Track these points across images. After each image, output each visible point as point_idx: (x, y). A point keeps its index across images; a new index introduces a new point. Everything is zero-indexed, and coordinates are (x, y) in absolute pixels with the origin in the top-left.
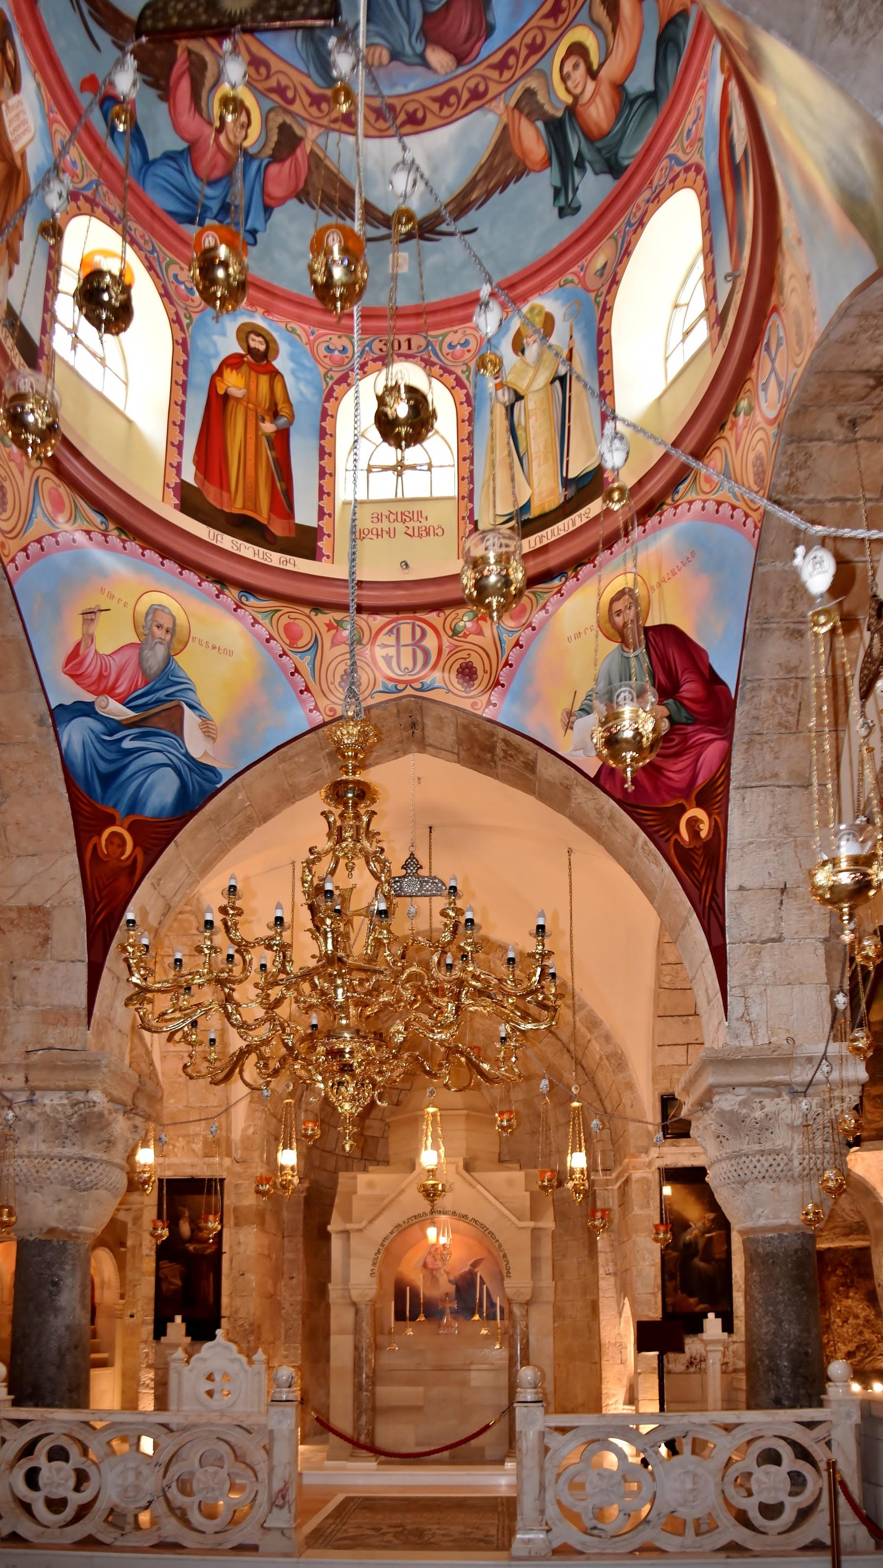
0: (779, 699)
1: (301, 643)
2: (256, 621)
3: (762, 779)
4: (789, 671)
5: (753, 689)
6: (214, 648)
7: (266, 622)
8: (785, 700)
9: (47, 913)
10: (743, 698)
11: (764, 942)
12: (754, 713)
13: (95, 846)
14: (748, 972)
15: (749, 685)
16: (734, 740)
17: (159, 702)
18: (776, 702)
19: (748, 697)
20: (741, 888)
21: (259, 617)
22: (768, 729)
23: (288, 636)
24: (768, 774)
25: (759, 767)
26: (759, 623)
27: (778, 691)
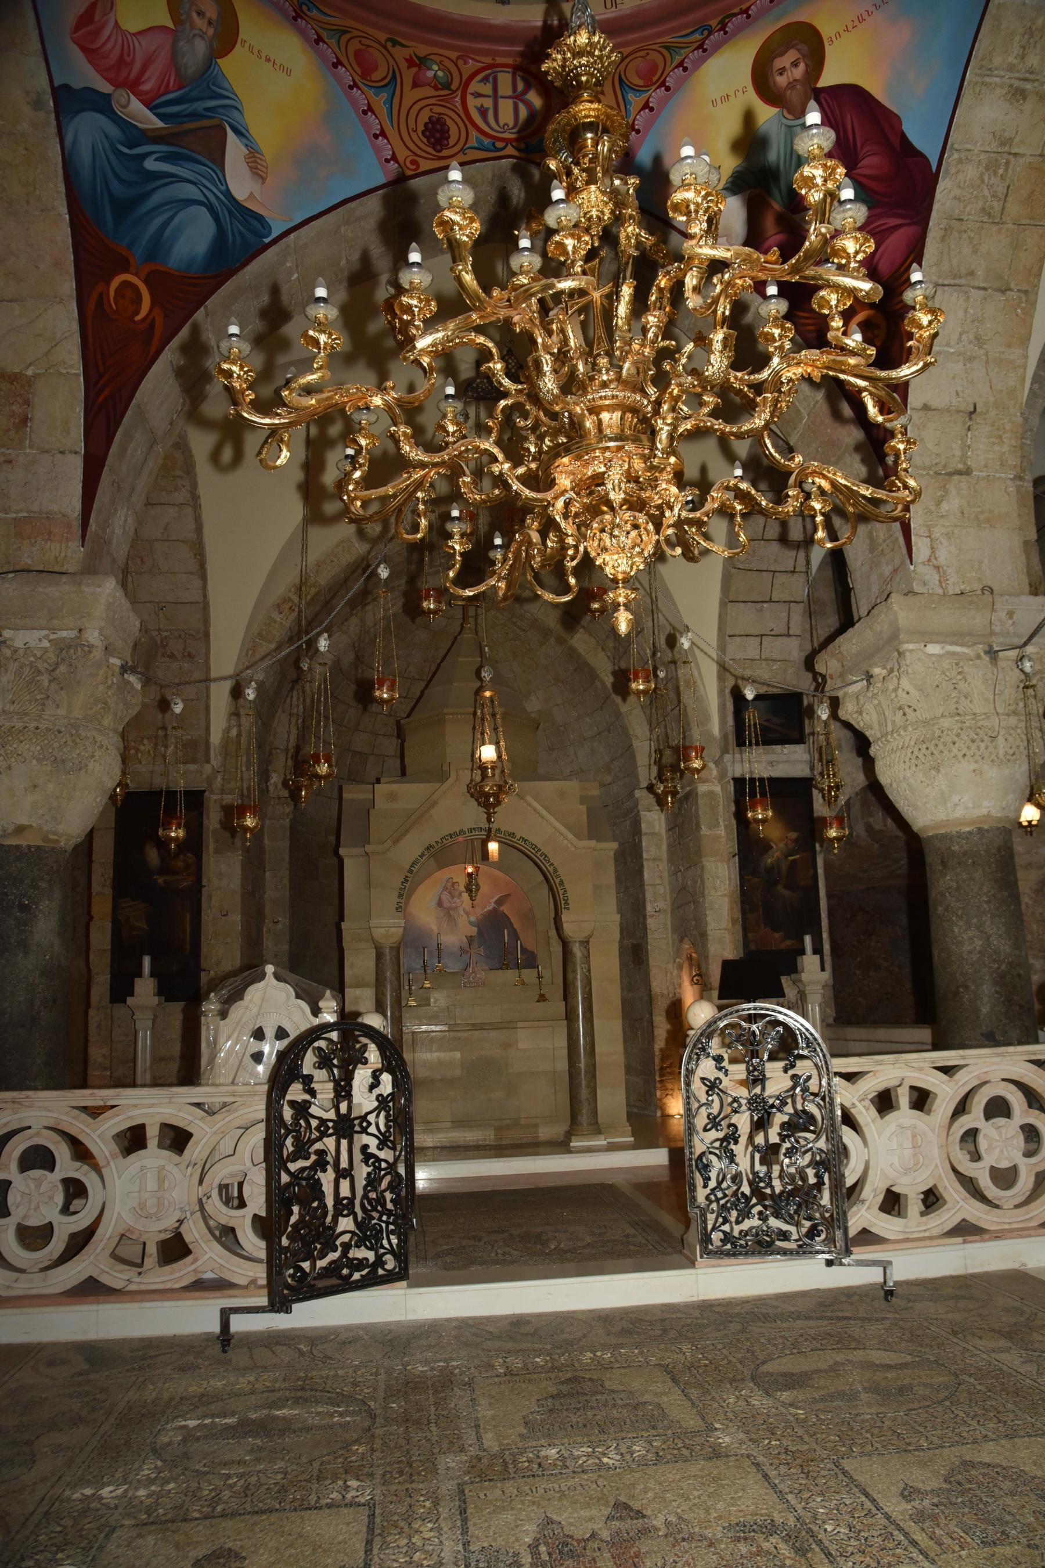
0: (986, 178)
1: (376, 76)
2: (319, 40)
3: (955, 277)
4: (1003, 144)
5: (960, 161)
6: (268, 60)
7: (333, 42)
8: (993, 180)
9: (29, 383)
10: (947, 171)
11: (950, 474)
12: (957, 192)
13: (101, 295)
14: (933, 508)
15: (956, 156)
16: (931, 224)
17: (194, 115)
18: (983, 181)
19: (953, 171)
20: (926, 408)
21: (324, 34)
22: (969, 214)
23: (359, 65)
24: (964, 271)
25: (955, 262)
26: (980, 75)
27: (987, 168)
